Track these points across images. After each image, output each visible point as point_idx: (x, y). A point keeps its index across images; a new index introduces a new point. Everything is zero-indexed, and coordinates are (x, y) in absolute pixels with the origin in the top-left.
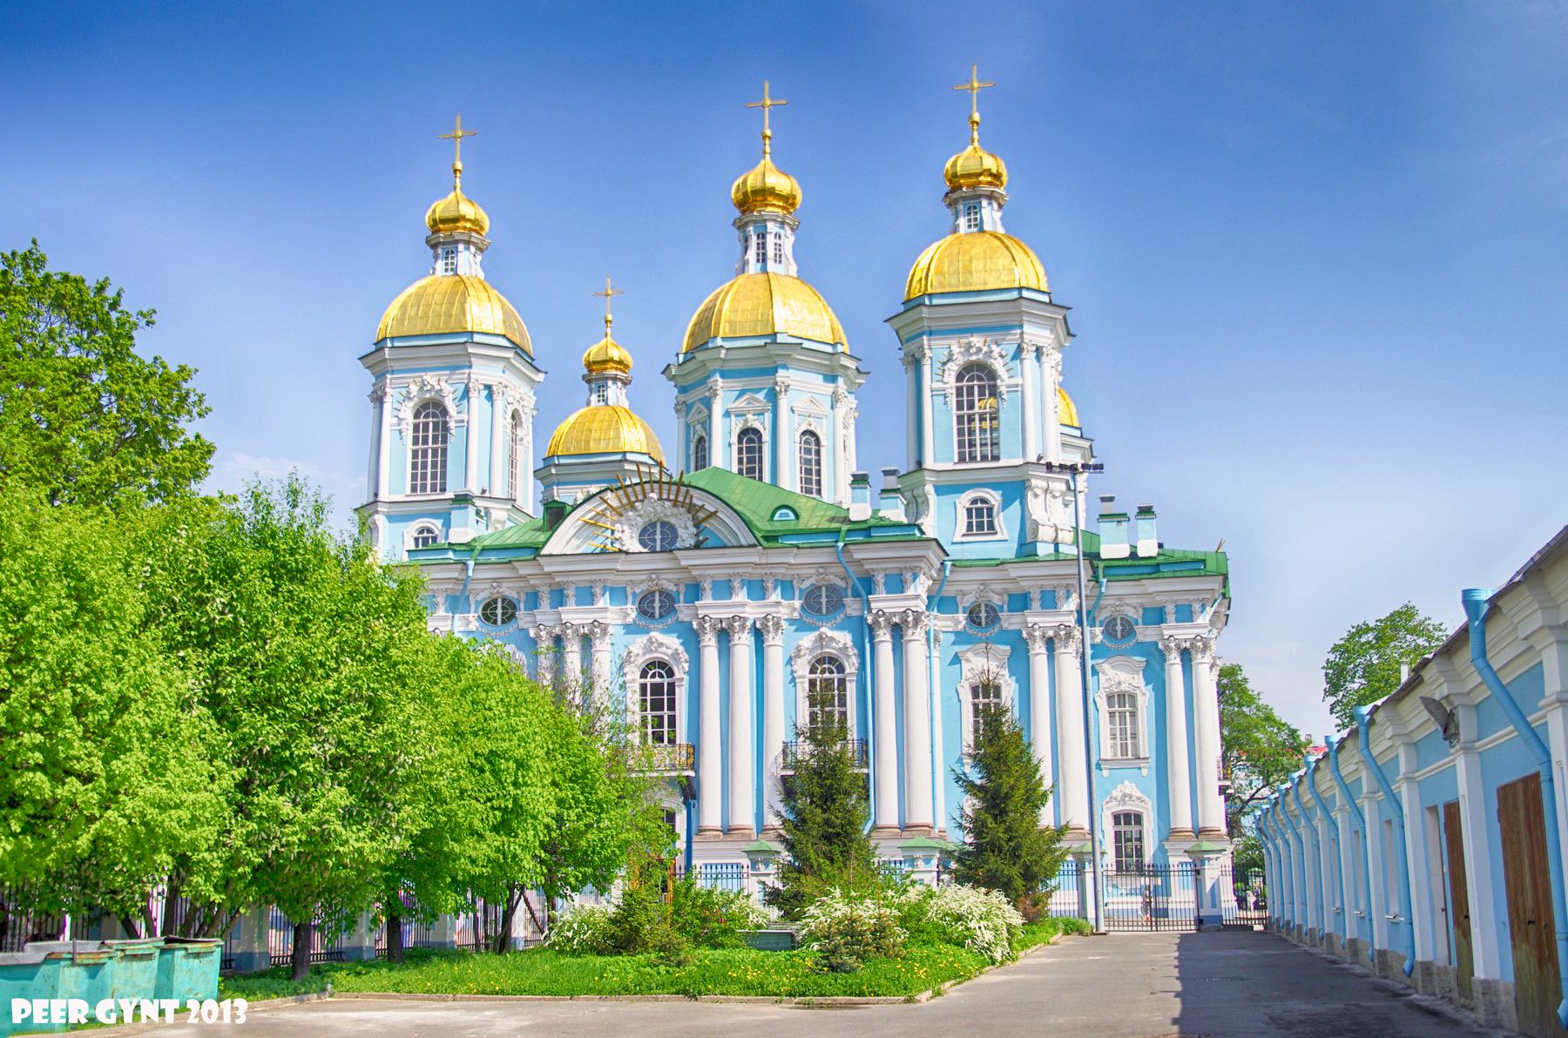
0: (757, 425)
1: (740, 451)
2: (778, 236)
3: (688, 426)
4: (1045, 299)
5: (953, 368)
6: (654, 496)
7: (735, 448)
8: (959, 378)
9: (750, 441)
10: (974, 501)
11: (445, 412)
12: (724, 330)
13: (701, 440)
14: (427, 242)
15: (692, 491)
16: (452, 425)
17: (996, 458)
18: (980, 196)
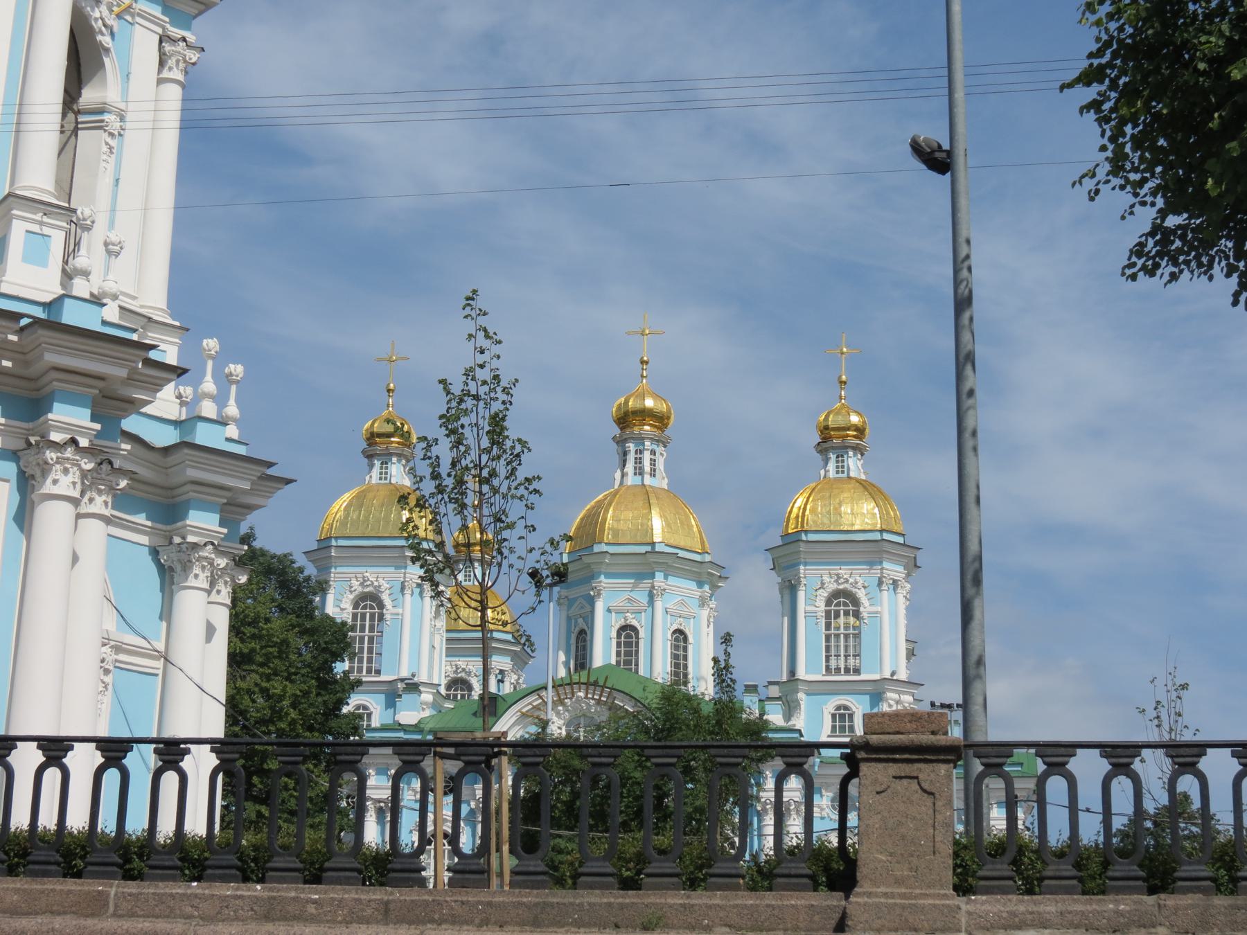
0: (634, 623)
1: (619, 645)
2: (653, 452)
3: (569, 618)
4: (900, 540)
5: (824, 594)
6: (581, 694)
7: (614, 642)
8: (828, 603)
9: (628, 636)
10: (838, 708)
11: (381, 605)
12: (608, 536)
13: (582, 632)
14: (363, 452)
15: (615, 694)
16: (387, 616)
17: (857, 671)
18: (847, 447)
